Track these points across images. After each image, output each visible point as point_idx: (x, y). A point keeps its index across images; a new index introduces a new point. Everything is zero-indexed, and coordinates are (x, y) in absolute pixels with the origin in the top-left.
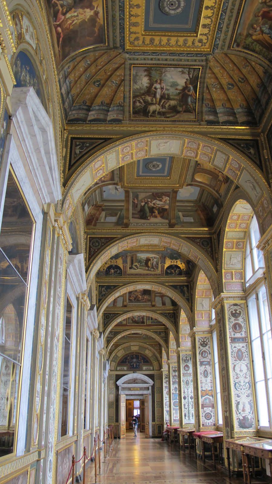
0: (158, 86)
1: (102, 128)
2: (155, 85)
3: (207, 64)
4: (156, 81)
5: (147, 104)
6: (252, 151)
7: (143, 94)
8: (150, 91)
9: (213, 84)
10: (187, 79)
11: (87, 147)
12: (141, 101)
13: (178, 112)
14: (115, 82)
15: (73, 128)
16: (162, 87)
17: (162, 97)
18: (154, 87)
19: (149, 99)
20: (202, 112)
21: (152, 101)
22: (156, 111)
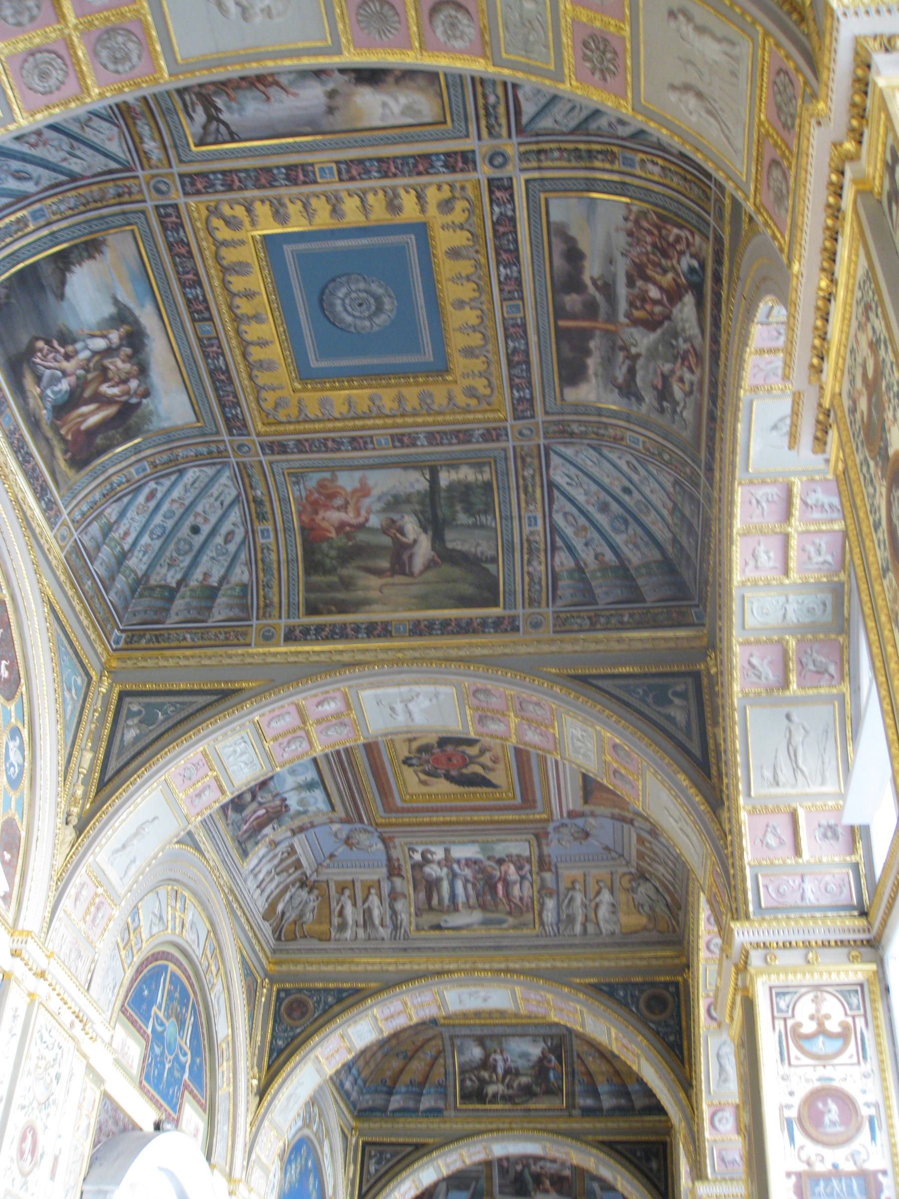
0: (499, 1057)
1: (412, 1126)
2: (493, 1056)
5: (483, 1083)
6: (654, 1165)
8: (486, 1064)
11: (388, 1161)
15: (366, 1125)
17: (507, 1071)
19: (485, 1075)
20: (573, 1094)
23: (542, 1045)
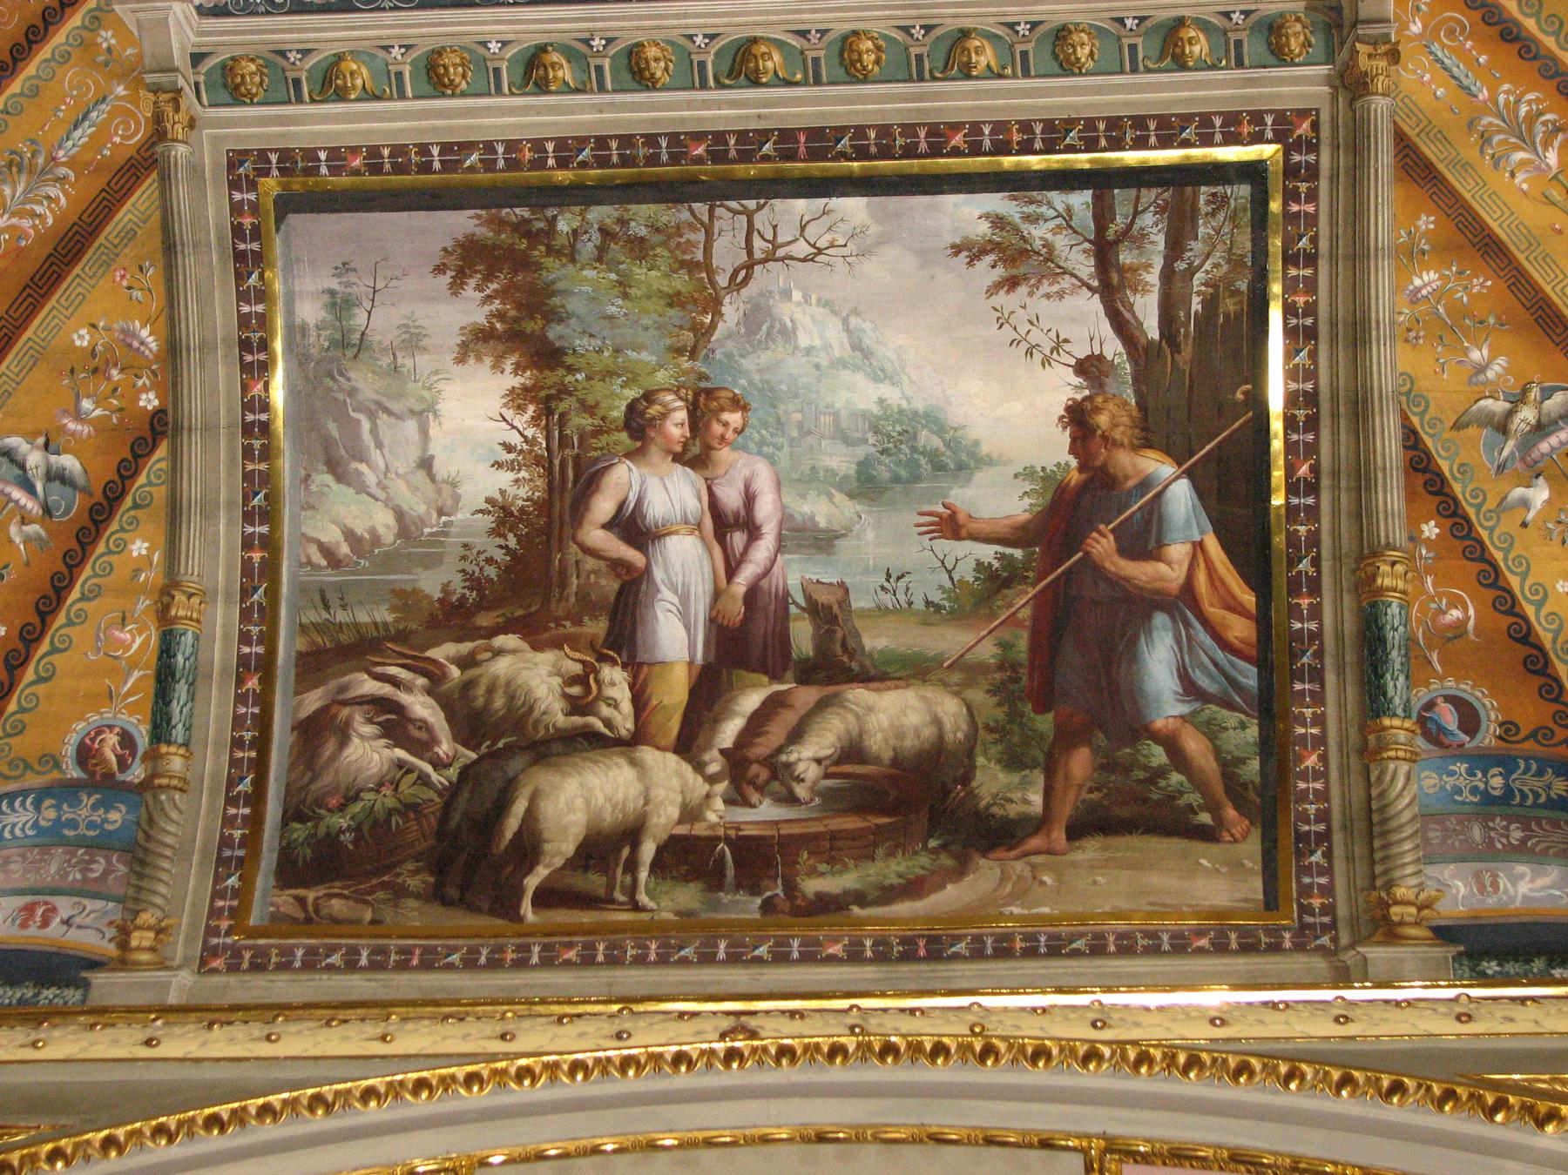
0: (669, 493)
2: (624, 481)
3: (1352, 86)
4: (639, 426)
5: (508, 743)
7: (453, 617)
8: (549, 568)
9: (1502, 427)
10: (1090, 367)
12: (422, 707)
13: (997, 834)
14: (35, 459)
16: (731, 498)
17: (743, 642)
18: (603, 506)
19: (535, 675)
20: (1372, 824)
21: (577, 706)
22: (632, 833)
23: (1083, 322)
